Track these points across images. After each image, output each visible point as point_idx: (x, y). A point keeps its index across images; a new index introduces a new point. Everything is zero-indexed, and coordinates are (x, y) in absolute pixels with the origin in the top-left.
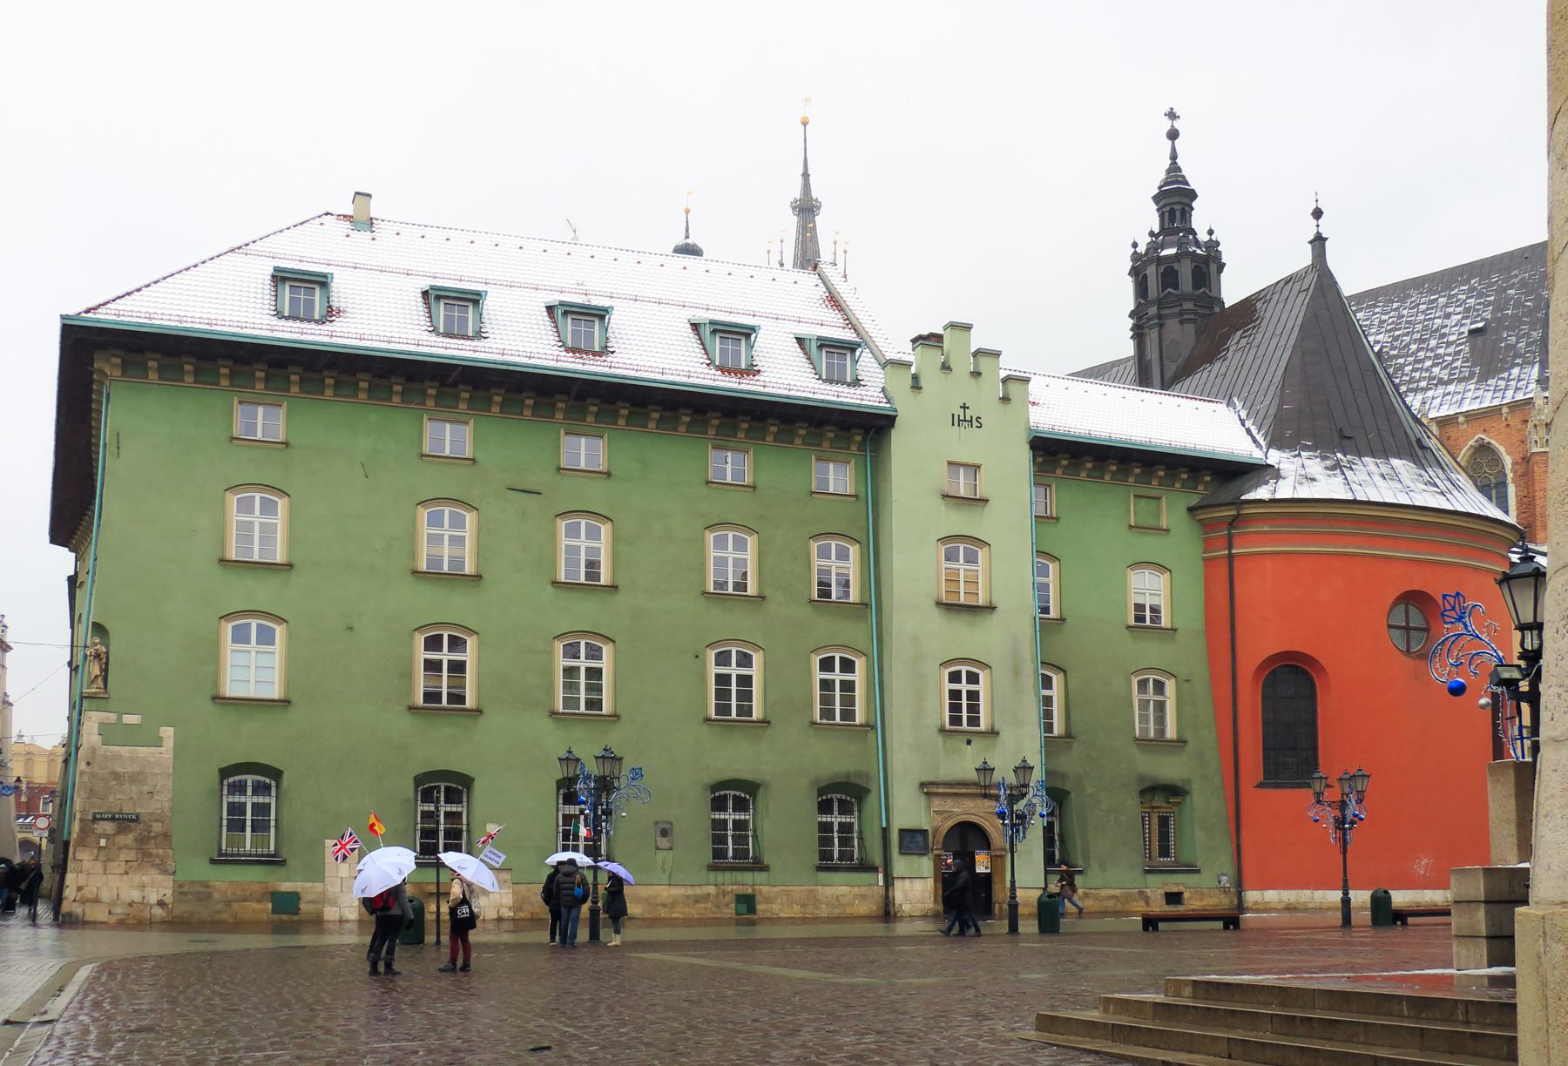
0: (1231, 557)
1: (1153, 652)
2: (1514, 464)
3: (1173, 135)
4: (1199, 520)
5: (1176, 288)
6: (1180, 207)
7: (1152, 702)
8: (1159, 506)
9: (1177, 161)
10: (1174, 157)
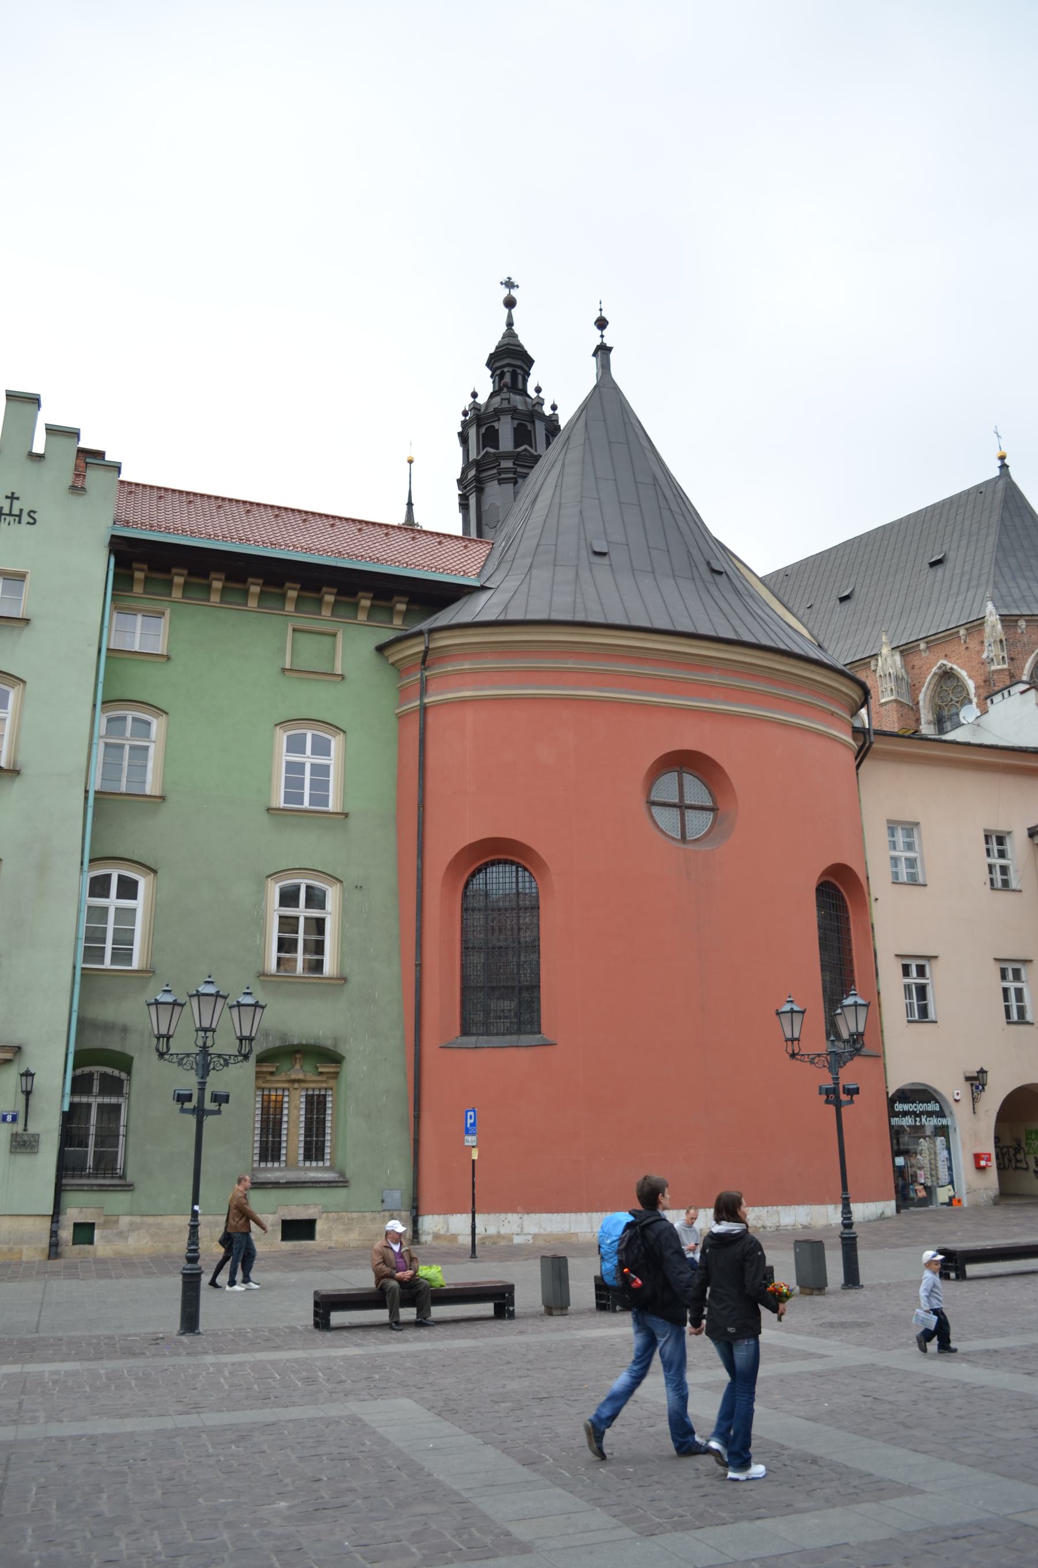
0: (424, 709)
2: (977, 688)
3: (510, 303)
4: (393, 664)
5: (497, 448)
6: (511, 369)
8: (334, 646)
9: (513, 328)
10: (510, 324)
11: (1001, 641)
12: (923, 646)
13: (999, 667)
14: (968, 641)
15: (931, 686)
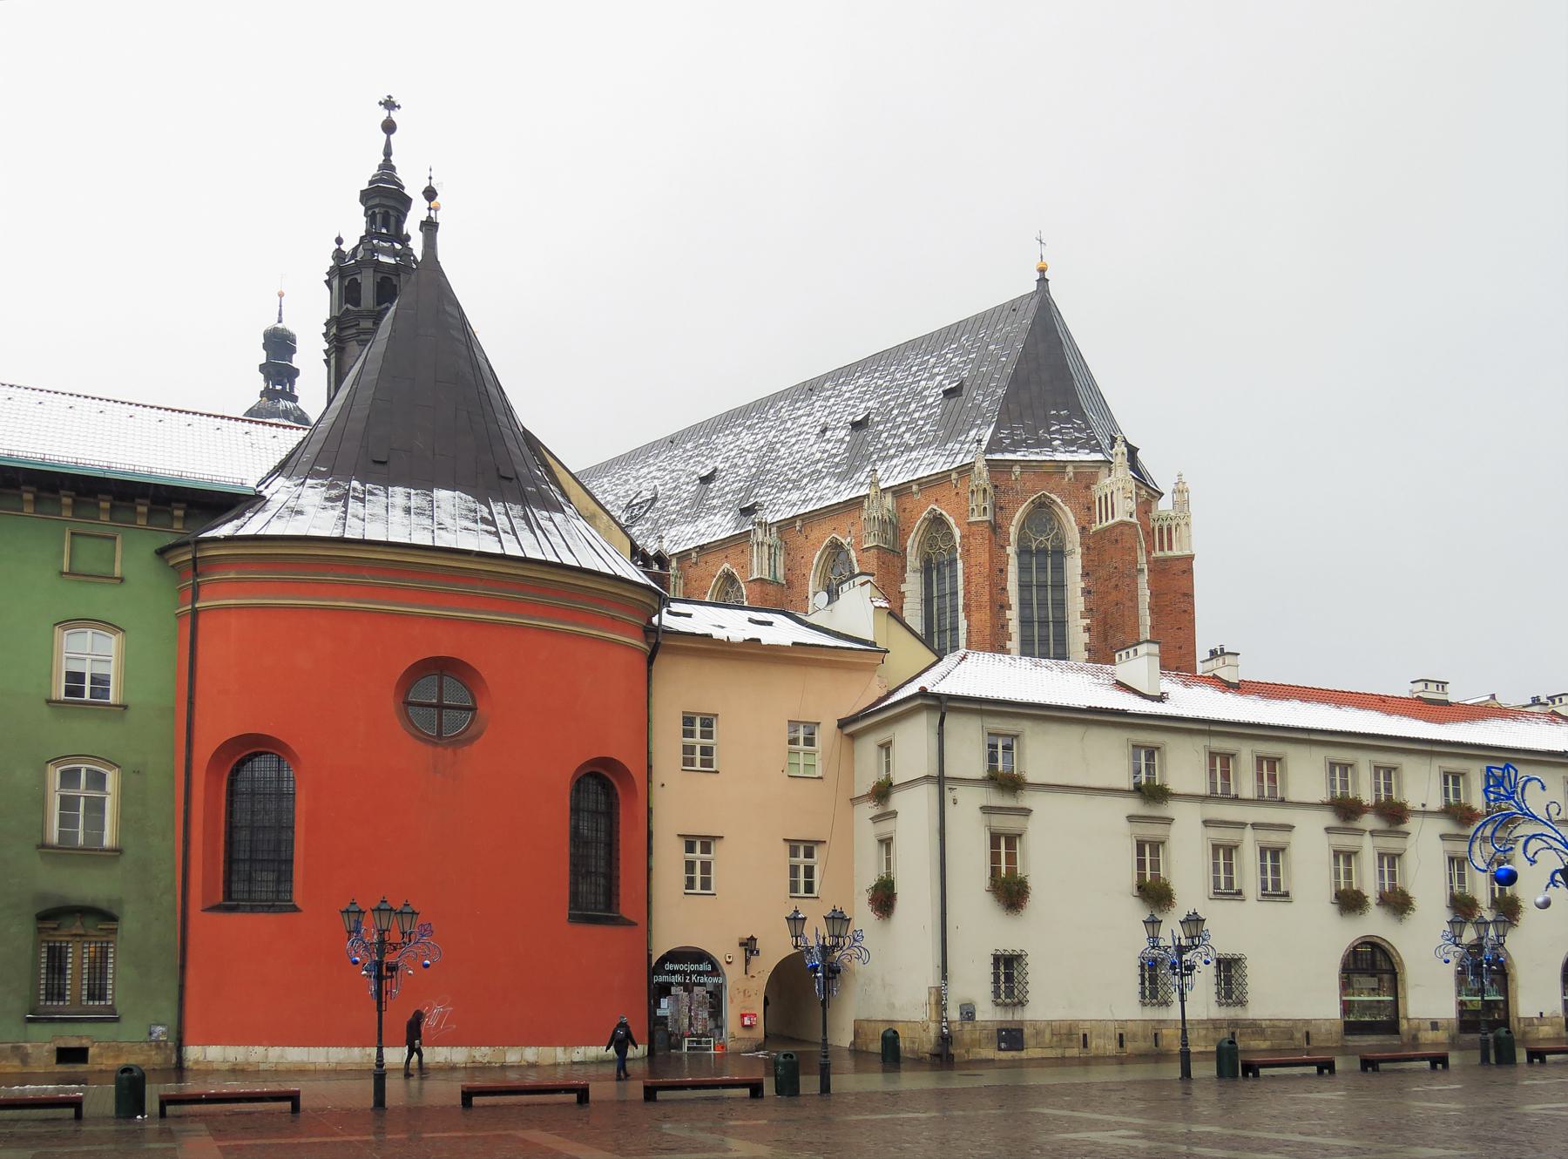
1: (84, 733)
2: (962, 537)
3: (389, 127)
7: (82, 800)
10: (388, 152)
11: (985, 490)
12: (915, 488)
13: (980, 519)
14: (959, 486)
15: (921, 532)
